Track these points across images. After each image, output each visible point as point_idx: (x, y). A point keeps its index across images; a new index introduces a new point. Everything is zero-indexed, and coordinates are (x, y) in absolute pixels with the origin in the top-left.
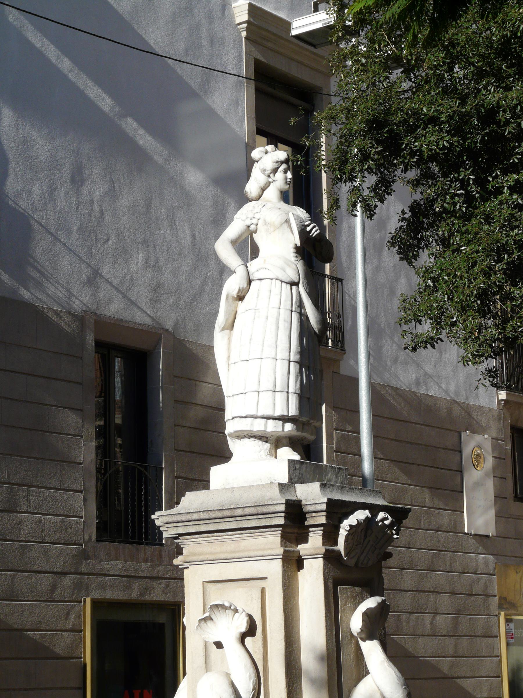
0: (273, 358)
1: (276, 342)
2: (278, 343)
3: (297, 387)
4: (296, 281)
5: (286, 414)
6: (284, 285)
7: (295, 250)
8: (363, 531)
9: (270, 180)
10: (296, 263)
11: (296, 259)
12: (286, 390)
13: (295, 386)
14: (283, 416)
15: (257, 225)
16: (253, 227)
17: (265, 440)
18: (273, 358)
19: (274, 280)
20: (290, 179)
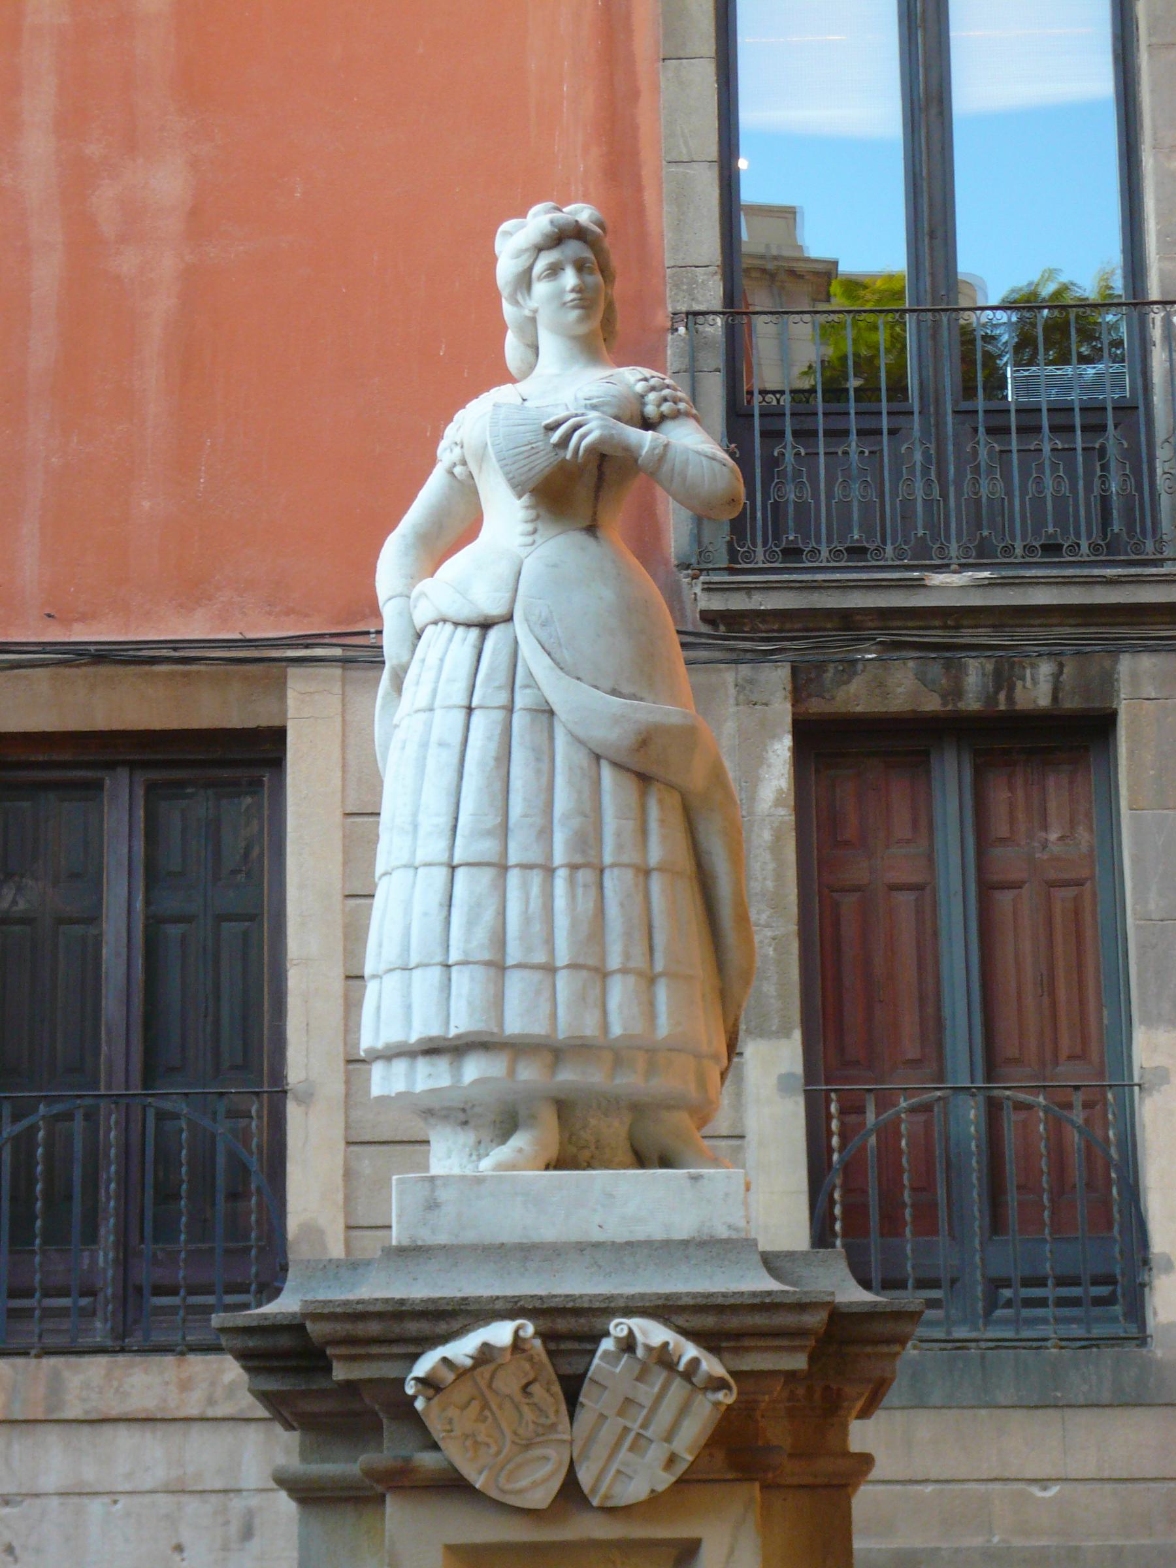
0: (405, 866)
1: (415, 814)
2: (421, 818)
3: (474, 944)
4: (494, 609)
5: (435, 1031)
6: (461, 630)
7: (532, 514)
8: (536, 1389)
9: (527, 313)
10: (523, 552)
11: (529, 539)
12: (438, 958)
13: (467, 941)
14: (431, 1039)
15: (464, 463)
16: (458, 470)
17: (462, 1117)
18: (405, 866)
19: (441, 624)
20: (573, 291)
